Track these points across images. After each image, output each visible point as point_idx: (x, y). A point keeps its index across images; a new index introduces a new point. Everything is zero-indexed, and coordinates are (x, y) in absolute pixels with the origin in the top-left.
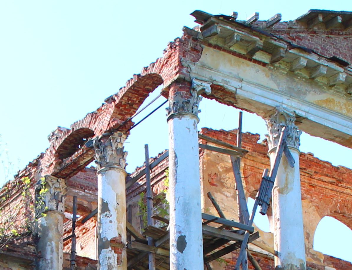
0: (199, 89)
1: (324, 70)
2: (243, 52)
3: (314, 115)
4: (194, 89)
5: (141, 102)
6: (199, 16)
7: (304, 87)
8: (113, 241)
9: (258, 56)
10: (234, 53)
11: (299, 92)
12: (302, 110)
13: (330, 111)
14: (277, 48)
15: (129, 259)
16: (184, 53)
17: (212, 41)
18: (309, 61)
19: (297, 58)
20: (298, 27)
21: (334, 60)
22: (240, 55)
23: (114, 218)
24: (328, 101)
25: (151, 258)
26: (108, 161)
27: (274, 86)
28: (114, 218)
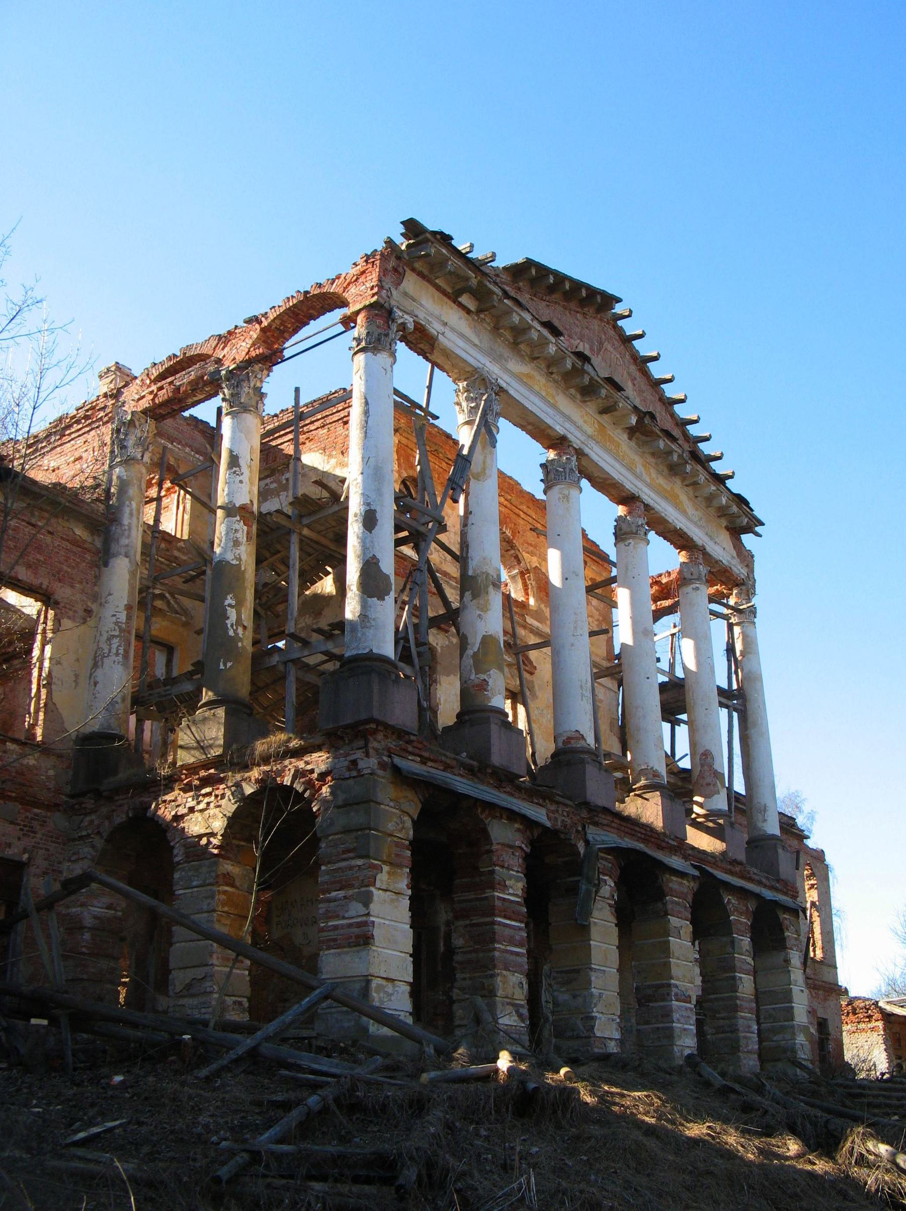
0: (400, 321)
1: (534, 335)
2: (449, 290)
4: (393, 320)
5: (296, 331)
6: (412, 227)
7: (507, 352)
8: (243, 508)
9: (465, 299)
10: (438, 288)
11: (501, 356)
13: (531, 389)
14: (492, 293)
15: (258, 536)
16: (384, 272)
17: (417, 265)
18: (522, 319)
19: (509, 312)
20: (504, 277)
21: (548, 325)
22: (444, 293)
23: (246, 477)
24: (528, 376)
25: (295, 539)
26: (242, 401)
27: (477, 342)
28: (246, 477)
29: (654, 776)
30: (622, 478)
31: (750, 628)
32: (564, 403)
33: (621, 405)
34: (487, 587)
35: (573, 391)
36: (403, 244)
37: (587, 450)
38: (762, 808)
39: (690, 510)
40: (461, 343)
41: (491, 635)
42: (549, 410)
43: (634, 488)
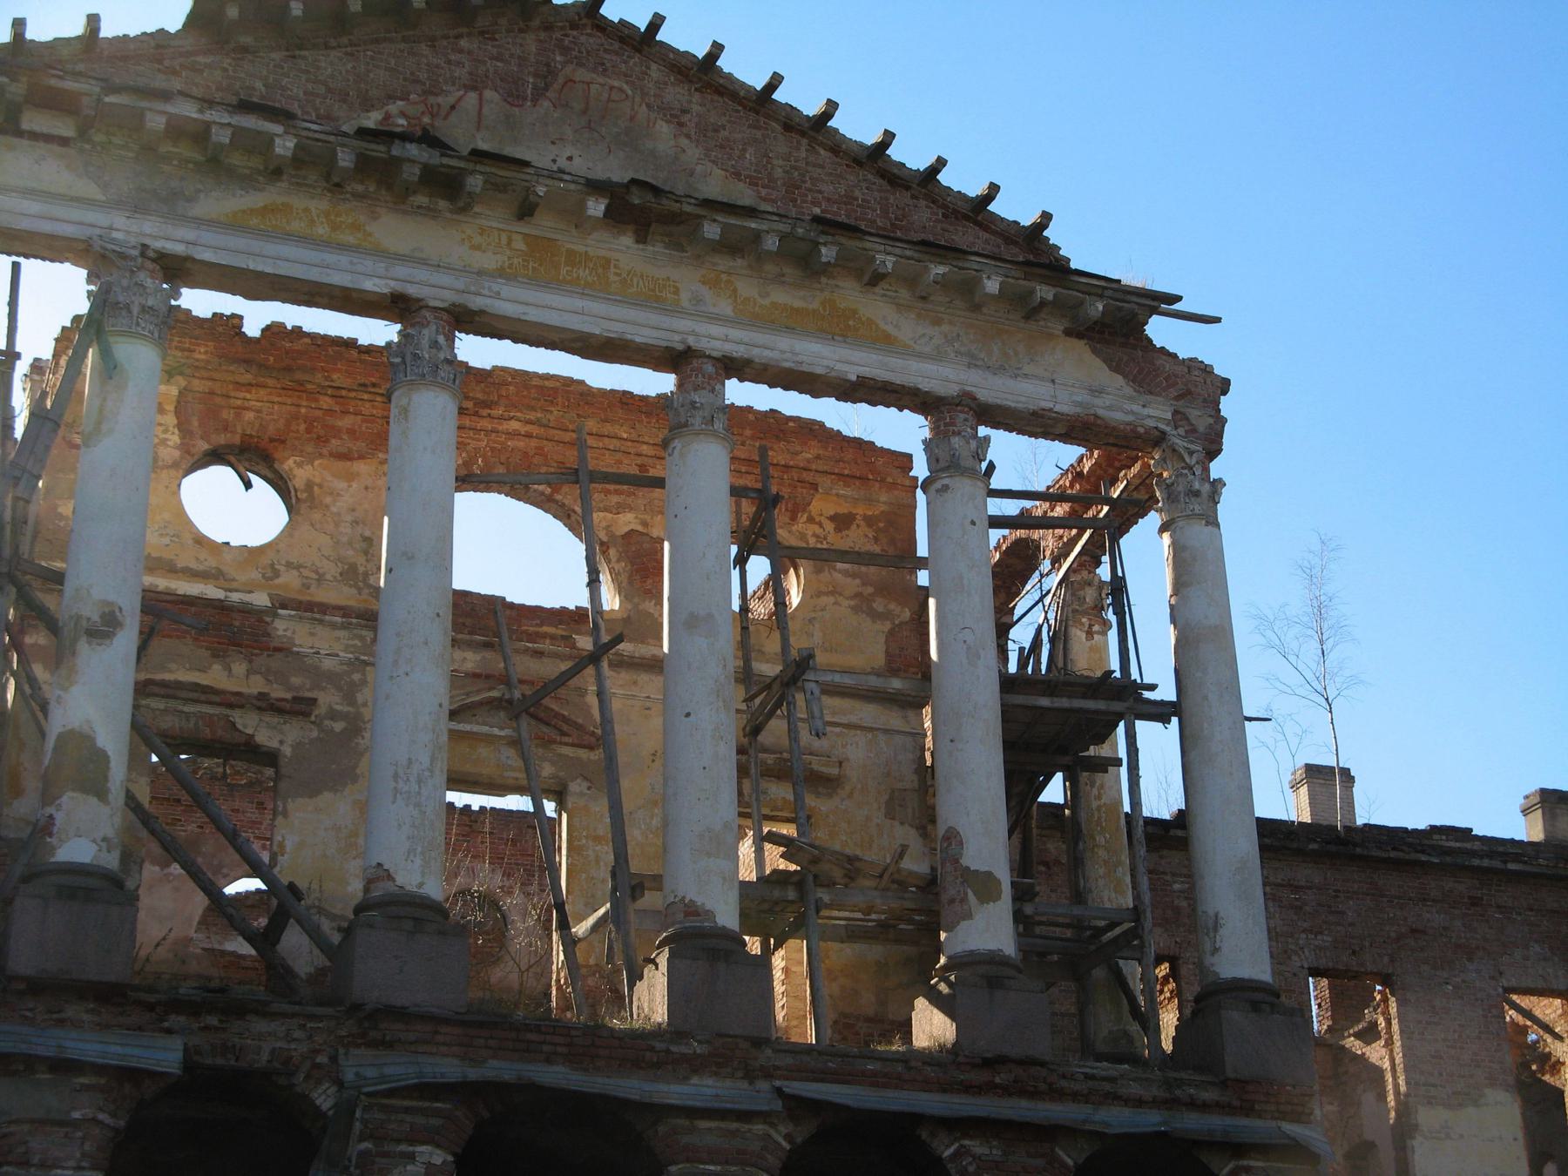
24: (265, 211)
29: (687, 914)
30: (606, 325)
31: (1196, 532)
32: (394, 230)
33: (541, 190)
34: (75, 641)
35: (421, 199)
38: (1211, 924)
39: (907, 328)
41: (72, 732)
42: (330, 258)
43: (655, 334)
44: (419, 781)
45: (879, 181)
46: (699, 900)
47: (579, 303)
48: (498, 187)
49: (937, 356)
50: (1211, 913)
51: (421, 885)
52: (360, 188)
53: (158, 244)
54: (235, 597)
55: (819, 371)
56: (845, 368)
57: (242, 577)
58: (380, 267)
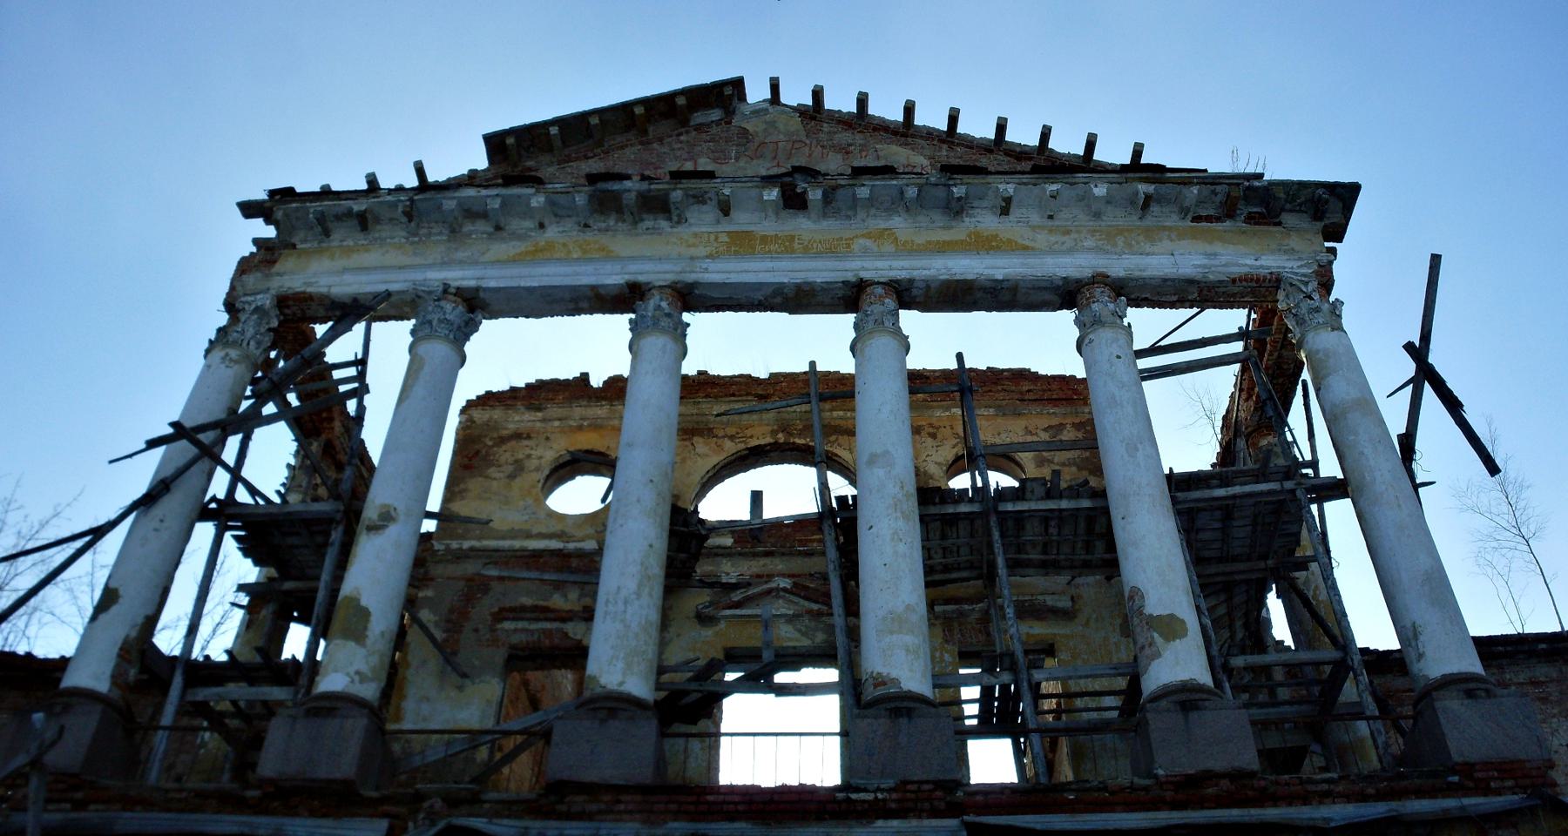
3: (494, 278)
12: (462, 277)
33: (727, 191)
36: (270, 232)
37: (690, 278)
39: (1042, 239)
40: (364, 278)
44: (626, 602)
45: (1007, 159)
46: (884, 671)
47: (769, 264)
48: (700, 199)
49: (1071, 251)
50: (1409, 625)
51: (621, 683)
52: (603, 225)
53: (455, 284)
54: (571, 546)
55: (970, 277)
56: (991, 272)
57: (579, 534)
58: (618, 267)
